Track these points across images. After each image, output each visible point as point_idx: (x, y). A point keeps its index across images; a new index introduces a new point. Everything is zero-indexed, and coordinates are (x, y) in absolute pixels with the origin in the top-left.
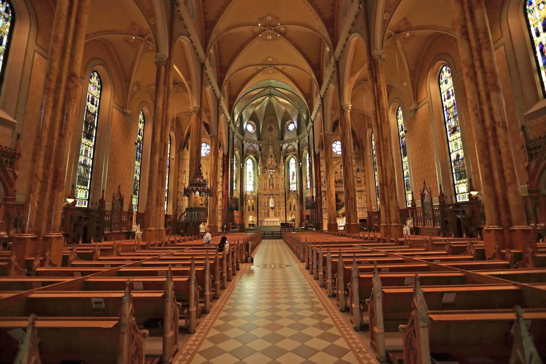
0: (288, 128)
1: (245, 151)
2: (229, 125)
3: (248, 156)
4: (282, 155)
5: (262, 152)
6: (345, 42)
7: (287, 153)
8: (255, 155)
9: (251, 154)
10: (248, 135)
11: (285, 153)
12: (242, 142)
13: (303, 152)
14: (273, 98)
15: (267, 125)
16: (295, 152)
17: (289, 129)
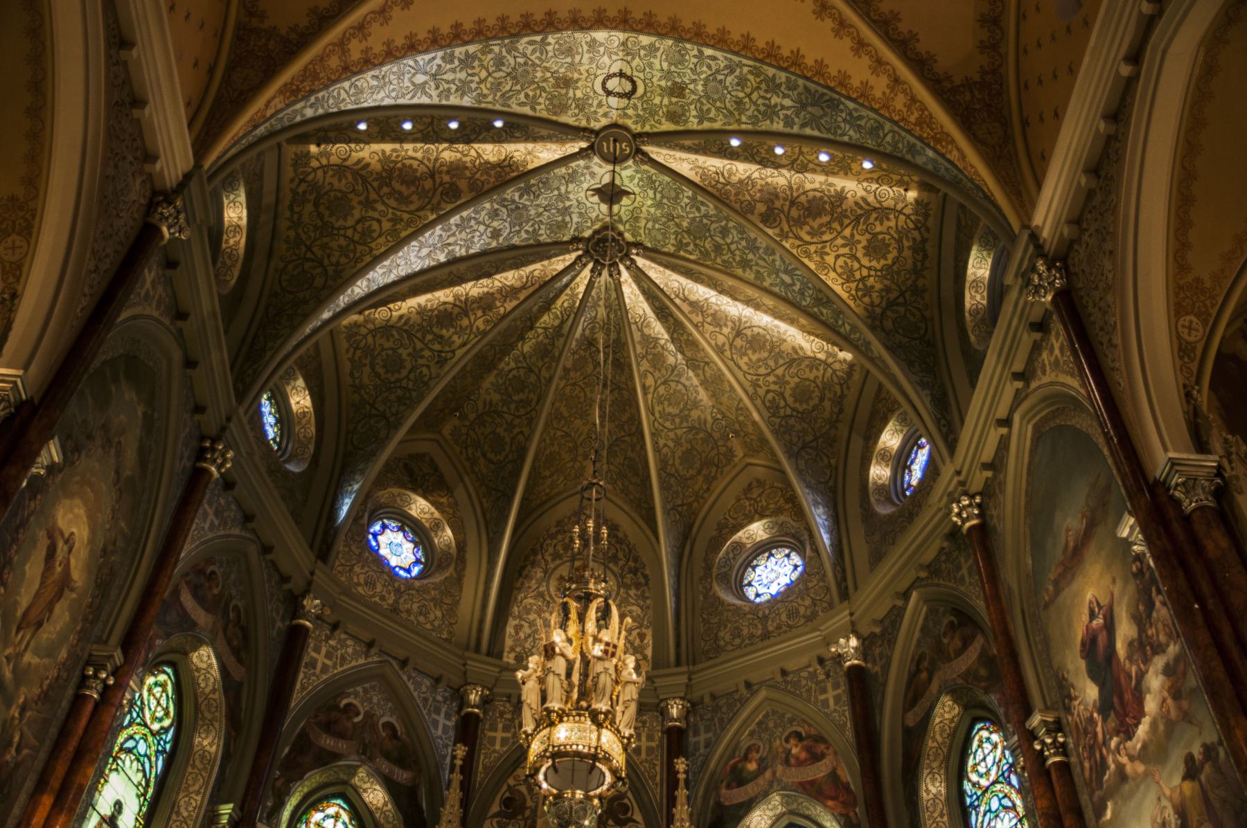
0: (739, 587)
1: (297, 698)
2: (151, 207)
3: (325, 759)
4: (682, 793)
5: (483, 761)
6: (1126, 70)
7: (738, 778)
8: (402, 776)
9: (367, 753)
10: (370, 583)
11: (713, 786)
12: (294, 605)
13: (914, 737)
14: (630, 291)
15: (556, 556)
16: (816, 758)
17: (751, 576)
